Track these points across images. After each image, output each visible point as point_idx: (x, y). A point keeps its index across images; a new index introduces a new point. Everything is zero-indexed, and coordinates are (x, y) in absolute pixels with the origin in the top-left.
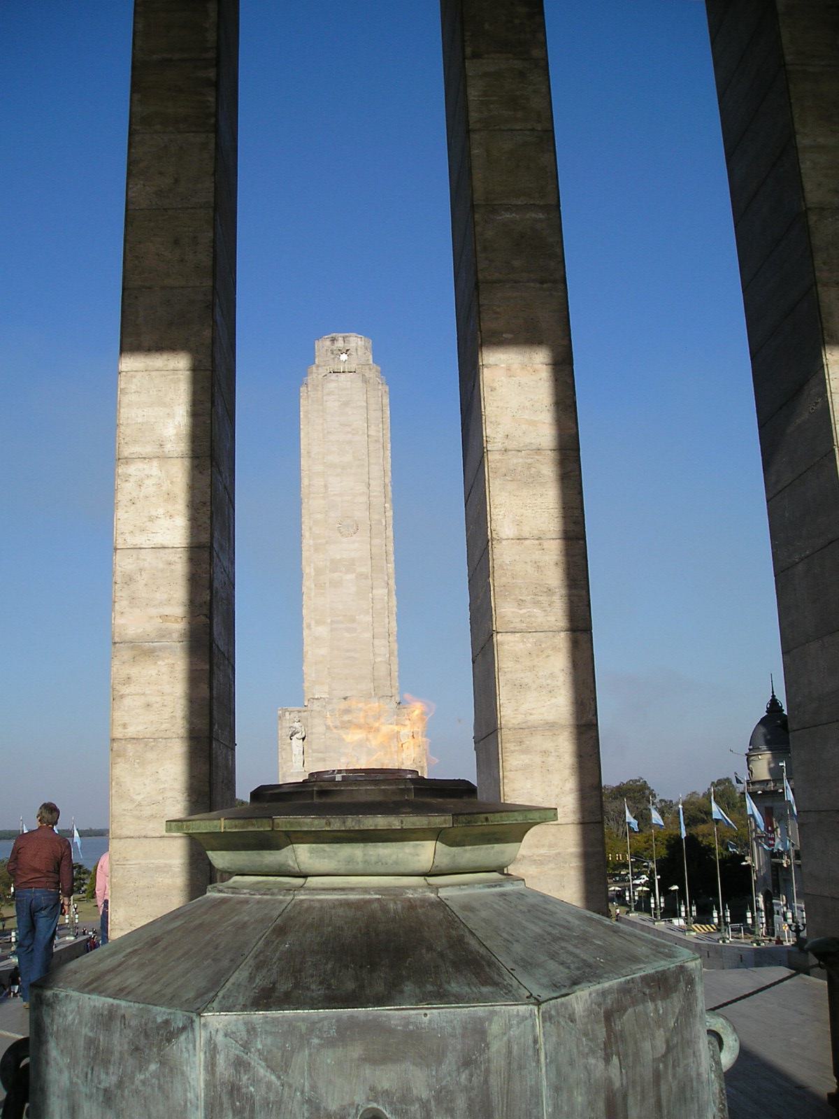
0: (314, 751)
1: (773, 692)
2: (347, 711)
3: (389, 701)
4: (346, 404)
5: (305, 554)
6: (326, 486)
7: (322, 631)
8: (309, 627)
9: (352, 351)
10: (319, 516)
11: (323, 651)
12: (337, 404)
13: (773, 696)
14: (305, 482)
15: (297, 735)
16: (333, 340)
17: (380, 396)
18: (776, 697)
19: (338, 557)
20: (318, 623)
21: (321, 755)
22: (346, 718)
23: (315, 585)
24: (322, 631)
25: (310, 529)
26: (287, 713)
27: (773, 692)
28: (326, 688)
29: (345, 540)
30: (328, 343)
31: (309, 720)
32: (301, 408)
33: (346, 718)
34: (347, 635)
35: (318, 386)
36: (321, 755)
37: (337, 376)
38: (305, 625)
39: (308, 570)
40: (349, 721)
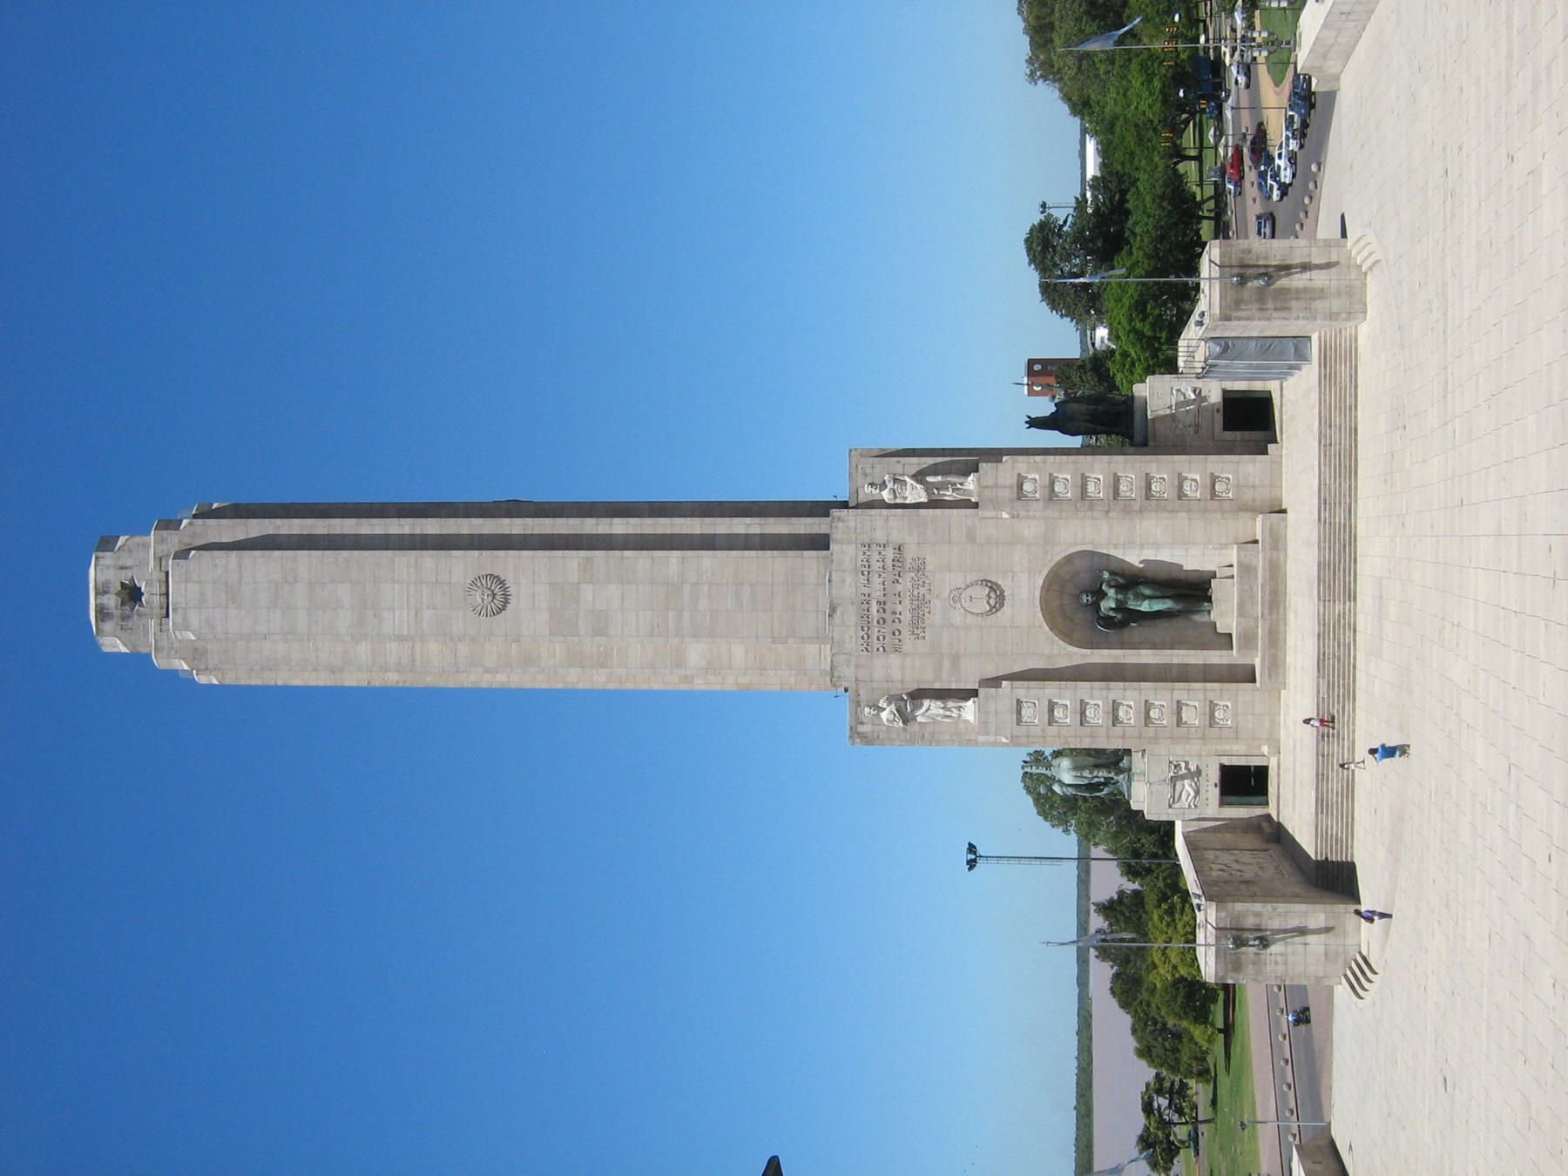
0: (938, 678)
3: (840, 525)
5: (541, 683)
6: (399, 638)
7: (696, 654)
8: (687, 679)
9: (125, 577)
10: (463, 649)
11: (738, 652)
12: (233, 611)
14: (392, 679)
19: (545, 616)
20: (679, 662)
21: (946, 663)
22: (874, 608)
23: (603, 665)
24: (696, 654)
25: (487, 671)
26: (861, 729)
28: (812, 649)
29: (513, 600)
30: (108, 626)
31: (875, 685)
32: (243, 682)
33: (874, 608)
34: (703, 604)
35: (196, 650)
38: (684, 687)
39: (573, 678)
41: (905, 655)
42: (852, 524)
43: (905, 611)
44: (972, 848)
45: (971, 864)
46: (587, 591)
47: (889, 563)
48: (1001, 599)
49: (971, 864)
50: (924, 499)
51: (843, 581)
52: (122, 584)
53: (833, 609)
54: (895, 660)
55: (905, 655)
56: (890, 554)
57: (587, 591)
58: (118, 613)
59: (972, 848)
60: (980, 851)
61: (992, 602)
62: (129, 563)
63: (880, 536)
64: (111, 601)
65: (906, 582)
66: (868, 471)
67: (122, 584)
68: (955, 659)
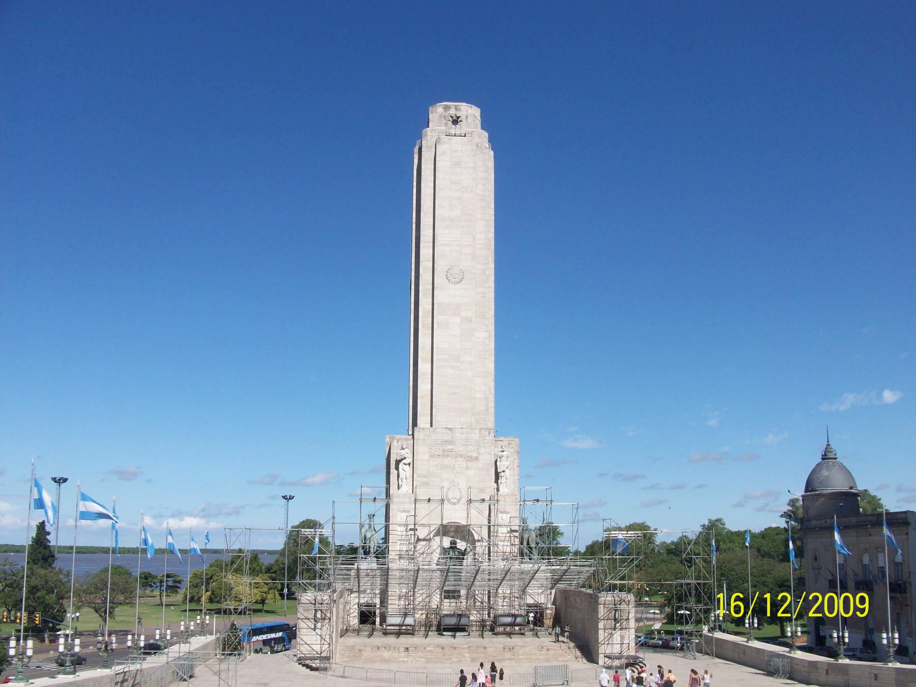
0: (419, 476)
2: (451, 442)
4: (457, 164)
9: (463, 118)
15: (404, 461)
16: (447, 108)
21: (425, 479)
22: (450, 447)
26: (395, 441)
33: (450, 447)
36: (425, 479)
40: (451, 450)
41: (429, 461)
42: (488, 438)
43: (447, 461)
44: (291, 498)
45: (285, 497)
46: (457, 320)
48: (455, 504)
49: (285, 497)
53: (450, 429)
54: (427, 456)
55: (429, 461)
56: (474, 455)
57: (457, 320)
58: (447, 114)
59: (291, 498)
60: (290, 501)
62: (469, 120)
63: (482, 450)
64: (452, 112)
65: (461, 462)
68: (426, 484)
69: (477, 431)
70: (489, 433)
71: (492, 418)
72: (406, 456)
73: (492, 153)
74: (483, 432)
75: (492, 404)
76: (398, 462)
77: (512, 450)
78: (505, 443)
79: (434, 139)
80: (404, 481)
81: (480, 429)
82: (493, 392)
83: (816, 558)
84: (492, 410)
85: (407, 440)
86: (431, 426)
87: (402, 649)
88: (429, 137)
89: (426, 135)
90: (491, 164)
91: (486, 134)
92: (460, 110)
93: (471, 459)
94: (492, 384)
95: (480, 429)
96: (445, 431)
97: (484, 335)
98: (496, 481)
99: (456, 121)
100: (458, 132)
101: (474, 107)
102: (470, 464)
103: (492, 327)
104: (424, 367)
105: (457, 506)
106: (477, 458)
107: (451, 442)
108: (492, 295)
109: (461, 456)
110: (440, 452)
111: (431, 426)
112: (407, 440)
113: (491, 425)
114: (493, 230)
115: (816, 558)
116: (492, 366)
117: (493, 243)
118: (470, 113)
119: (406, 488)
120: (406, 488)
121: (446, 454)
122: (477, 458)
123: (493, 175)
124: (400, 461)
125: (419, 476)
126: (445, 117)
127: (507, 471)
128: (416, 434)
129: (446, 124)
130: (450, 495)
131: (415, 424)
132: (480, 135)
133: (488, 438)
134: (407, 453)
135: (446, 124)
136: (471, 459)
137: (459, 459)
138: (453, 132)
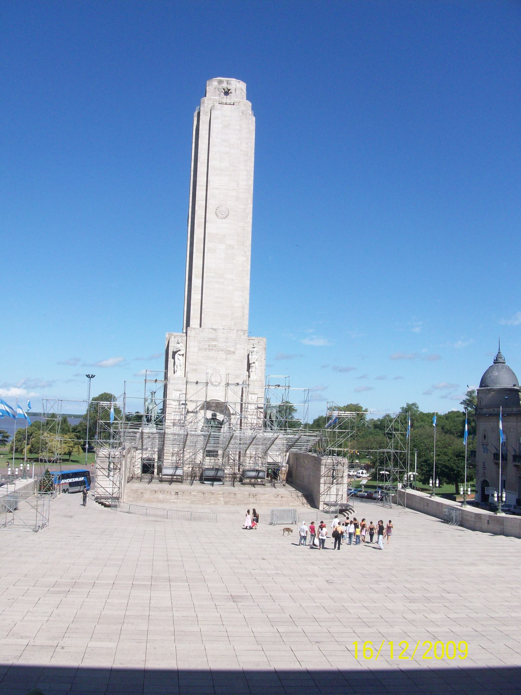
0: (190, 364)
1: (499, 350)
2: (215, 340)
3: (243, 333)
9: (233, 90)
13: (499, 352)
15: (179, 353)
16: (220, 82)
17: (251, 122)
18: (503, 353)
21: (194, 367)
22: (214, 343)
26: (173, 337)
27: (499, 350)
33: (214, 343)
37: (222, 106)
40: (215, 346)
42: (243, 337)
43: (212, 354)
47: (229, 349)
48: (216, 386)
50: (250, 362)
51: (224, 333)
52: (230, 90)
53: (214, 330)
56: (232, 349)
58: (220, 87)
61: (214, 383)
62: (237, 92)
63: (238, 346)
64: (225, 85)
65: (223, 355)
66: (260, 344)
67: (229, 90)
68: (195, 370)
69: (235, 331)
70: (244, 333)
71: (246, 322)
72: (181, 348)
73: (254, 119)
74: (239, 333)
75: (247, 311)
76: (174, 353)
77: (261, 347)
78: (256, 342)
79: (210, 106)
80: (179, 367)
81: (237, 331)
82: (248, 302)
83: (485, 436)
84: (247, 316)
85: (181, 336)
86: (200, 326)
87: (173, 493)
88: (206, 104)
89: (204, 103)
90: (253, 127)
91: (250, 104)
92: (230, 84)
93: (229, 352)
94: (248, 296)
95: (237, 331)
96: (210, 331)
97: (243, 259)
98: (248, 370)
99: (227, 93)
100: (228, 101)
101: (241, 82)
102: (229, 356)
103: (249, 253)
104: (196, 282)
105: (218, 387)
106: (234, 352)
107: (215, 340)
108: (249, 229)
109: (222, 350)
110: (207, 346)
111: (200, 326)
112: (181, 336)
113: (246, 327)
114: (252, 178)
115: (485, 436)
116: (248, 282)
117: (252, 188)
118: (238, 86)
119: (180, 373)
120: (180, 373)
121: (211, 348)
122: (234, 352)
123: (254, 136)
124: (176, 352)
125: (190, 364)
126: (219, 89)
127: (256, 362)
128: (188, 332)
129: (219, 94)
130: (213, 380)
131: (188, 325)
132: (245, 105)
133: (243, 337)
134: (181, 346)
135: (219, 94)
136: (229, 352)
137: (220, 352)
138: (224, 101)
